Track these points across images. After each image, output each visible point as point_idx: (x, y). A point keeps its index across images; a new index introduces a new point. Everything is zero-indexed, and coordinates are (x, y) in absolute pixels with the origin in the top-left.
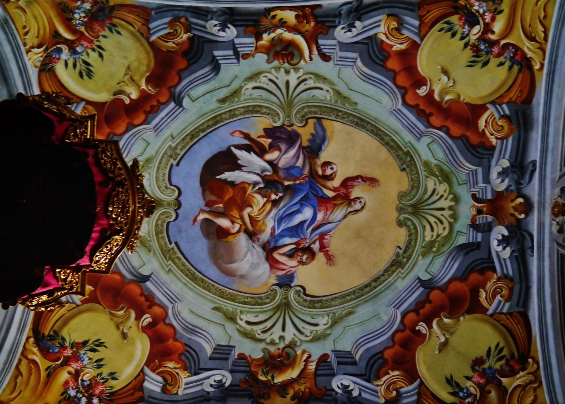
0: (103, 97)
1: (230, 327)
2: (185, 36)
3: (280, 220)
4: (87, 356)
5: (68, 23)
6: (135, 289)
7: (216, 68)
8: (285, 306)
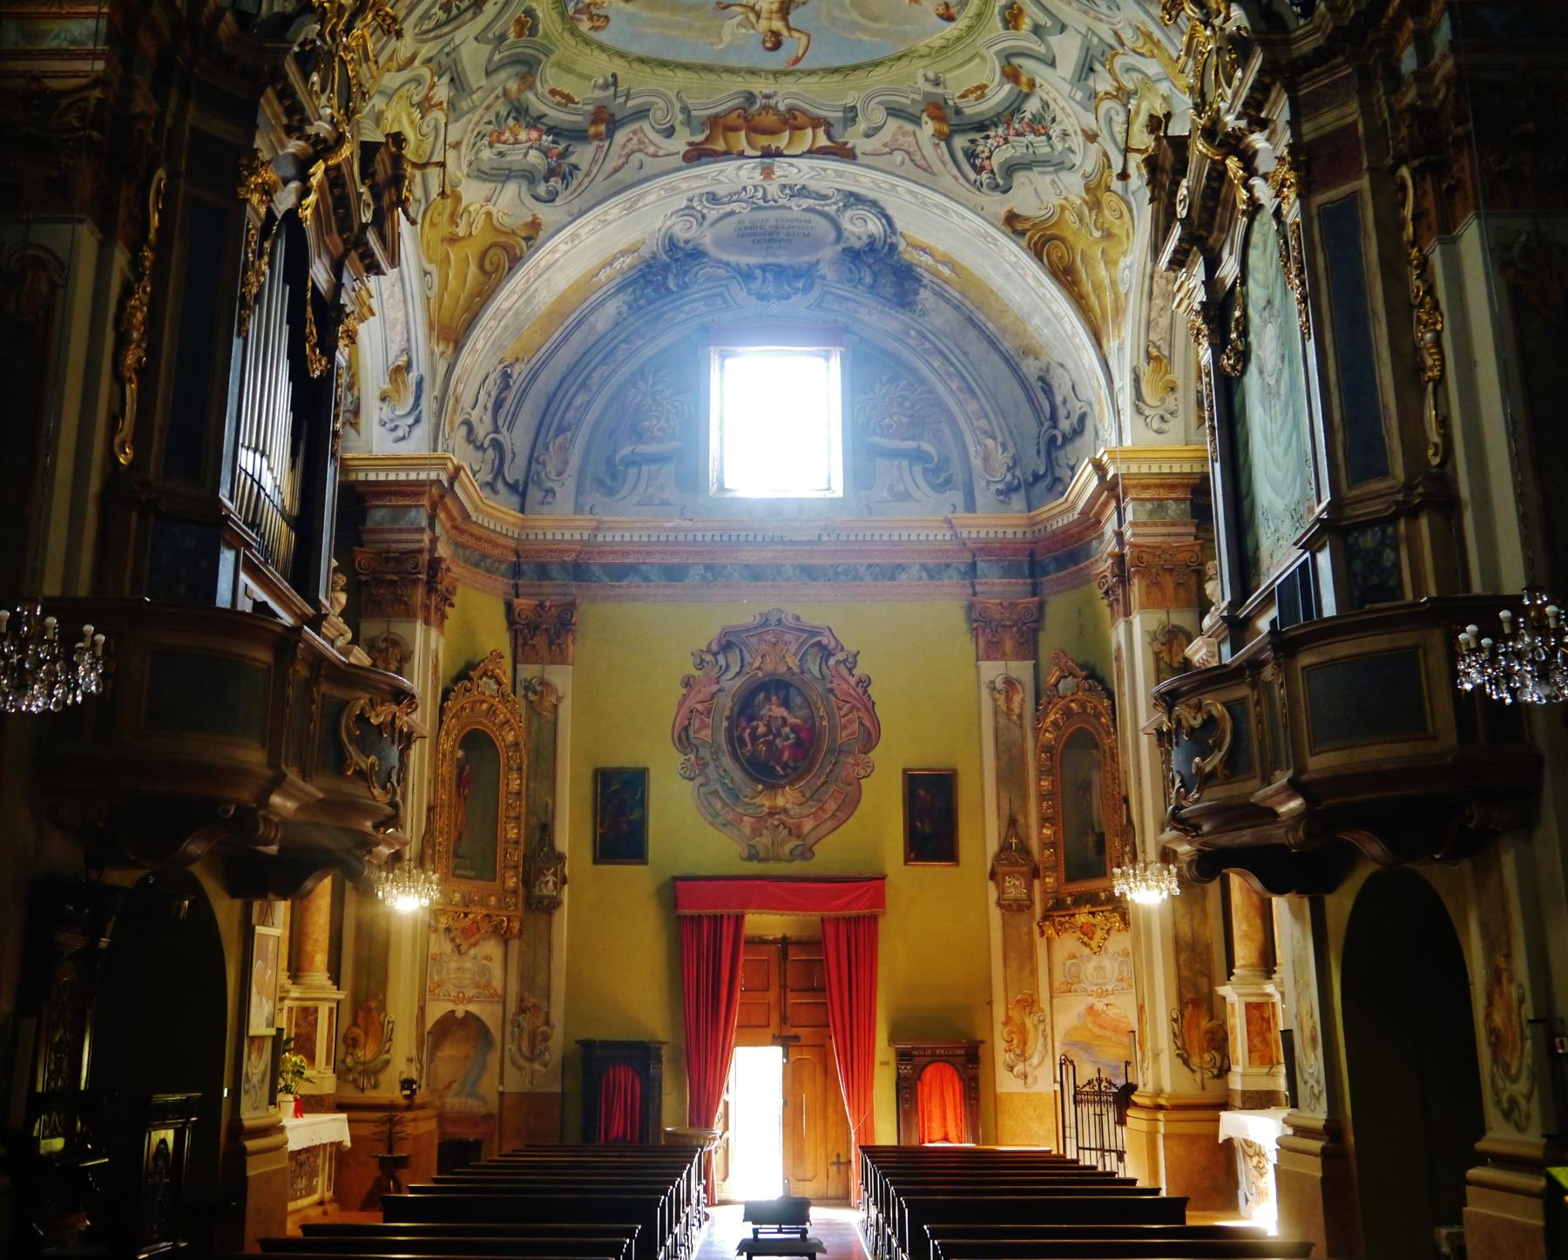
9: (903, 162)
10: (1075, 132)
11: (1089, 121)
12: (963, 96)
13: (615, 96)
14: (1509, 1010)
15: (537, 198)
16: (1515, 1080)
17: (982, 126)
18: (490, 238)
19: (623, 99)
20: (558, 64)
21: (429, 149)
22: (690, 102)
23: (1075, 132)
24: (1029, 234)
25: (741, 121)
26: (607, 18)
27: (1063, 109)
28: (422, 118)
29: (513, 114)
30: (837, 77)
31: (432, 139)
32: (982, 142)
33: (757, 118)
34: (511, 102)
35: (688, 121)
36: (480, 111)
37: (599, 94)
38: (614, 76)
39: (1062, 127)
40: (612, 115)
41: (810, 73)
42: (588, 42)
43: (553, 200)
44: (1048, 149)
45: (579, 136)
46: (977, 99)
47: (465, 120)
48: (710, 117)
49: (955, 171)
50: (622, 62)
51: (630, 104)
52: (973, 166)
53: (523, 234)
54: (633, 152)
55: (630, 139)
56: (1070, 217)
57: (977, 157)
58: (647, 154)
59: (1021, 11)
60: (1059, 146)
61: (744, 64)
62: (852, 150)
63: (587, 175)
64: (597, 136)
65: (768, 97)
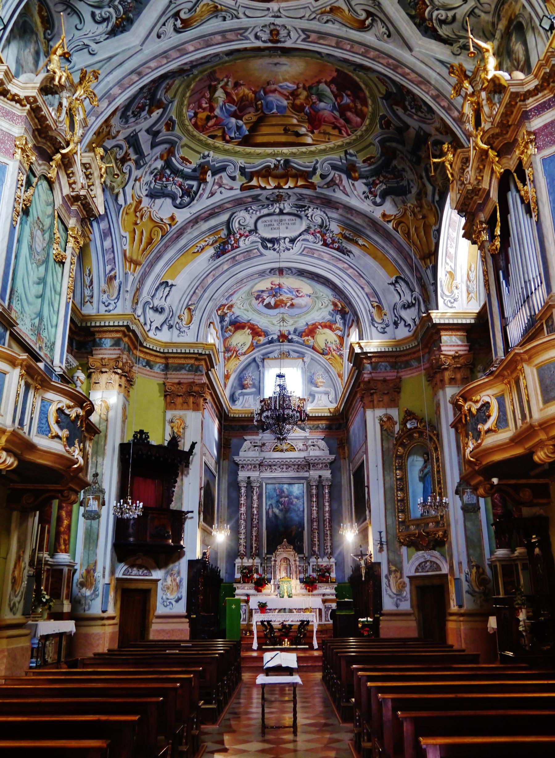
0: (251, 337)
1: (323, 310)
2: (230, 327)
4: (329, 345)
5: (231, 356)
6: (310, 327)
7: (238, 316)
8: (316, 297)
14: (20, 572)
16: (16, 597)
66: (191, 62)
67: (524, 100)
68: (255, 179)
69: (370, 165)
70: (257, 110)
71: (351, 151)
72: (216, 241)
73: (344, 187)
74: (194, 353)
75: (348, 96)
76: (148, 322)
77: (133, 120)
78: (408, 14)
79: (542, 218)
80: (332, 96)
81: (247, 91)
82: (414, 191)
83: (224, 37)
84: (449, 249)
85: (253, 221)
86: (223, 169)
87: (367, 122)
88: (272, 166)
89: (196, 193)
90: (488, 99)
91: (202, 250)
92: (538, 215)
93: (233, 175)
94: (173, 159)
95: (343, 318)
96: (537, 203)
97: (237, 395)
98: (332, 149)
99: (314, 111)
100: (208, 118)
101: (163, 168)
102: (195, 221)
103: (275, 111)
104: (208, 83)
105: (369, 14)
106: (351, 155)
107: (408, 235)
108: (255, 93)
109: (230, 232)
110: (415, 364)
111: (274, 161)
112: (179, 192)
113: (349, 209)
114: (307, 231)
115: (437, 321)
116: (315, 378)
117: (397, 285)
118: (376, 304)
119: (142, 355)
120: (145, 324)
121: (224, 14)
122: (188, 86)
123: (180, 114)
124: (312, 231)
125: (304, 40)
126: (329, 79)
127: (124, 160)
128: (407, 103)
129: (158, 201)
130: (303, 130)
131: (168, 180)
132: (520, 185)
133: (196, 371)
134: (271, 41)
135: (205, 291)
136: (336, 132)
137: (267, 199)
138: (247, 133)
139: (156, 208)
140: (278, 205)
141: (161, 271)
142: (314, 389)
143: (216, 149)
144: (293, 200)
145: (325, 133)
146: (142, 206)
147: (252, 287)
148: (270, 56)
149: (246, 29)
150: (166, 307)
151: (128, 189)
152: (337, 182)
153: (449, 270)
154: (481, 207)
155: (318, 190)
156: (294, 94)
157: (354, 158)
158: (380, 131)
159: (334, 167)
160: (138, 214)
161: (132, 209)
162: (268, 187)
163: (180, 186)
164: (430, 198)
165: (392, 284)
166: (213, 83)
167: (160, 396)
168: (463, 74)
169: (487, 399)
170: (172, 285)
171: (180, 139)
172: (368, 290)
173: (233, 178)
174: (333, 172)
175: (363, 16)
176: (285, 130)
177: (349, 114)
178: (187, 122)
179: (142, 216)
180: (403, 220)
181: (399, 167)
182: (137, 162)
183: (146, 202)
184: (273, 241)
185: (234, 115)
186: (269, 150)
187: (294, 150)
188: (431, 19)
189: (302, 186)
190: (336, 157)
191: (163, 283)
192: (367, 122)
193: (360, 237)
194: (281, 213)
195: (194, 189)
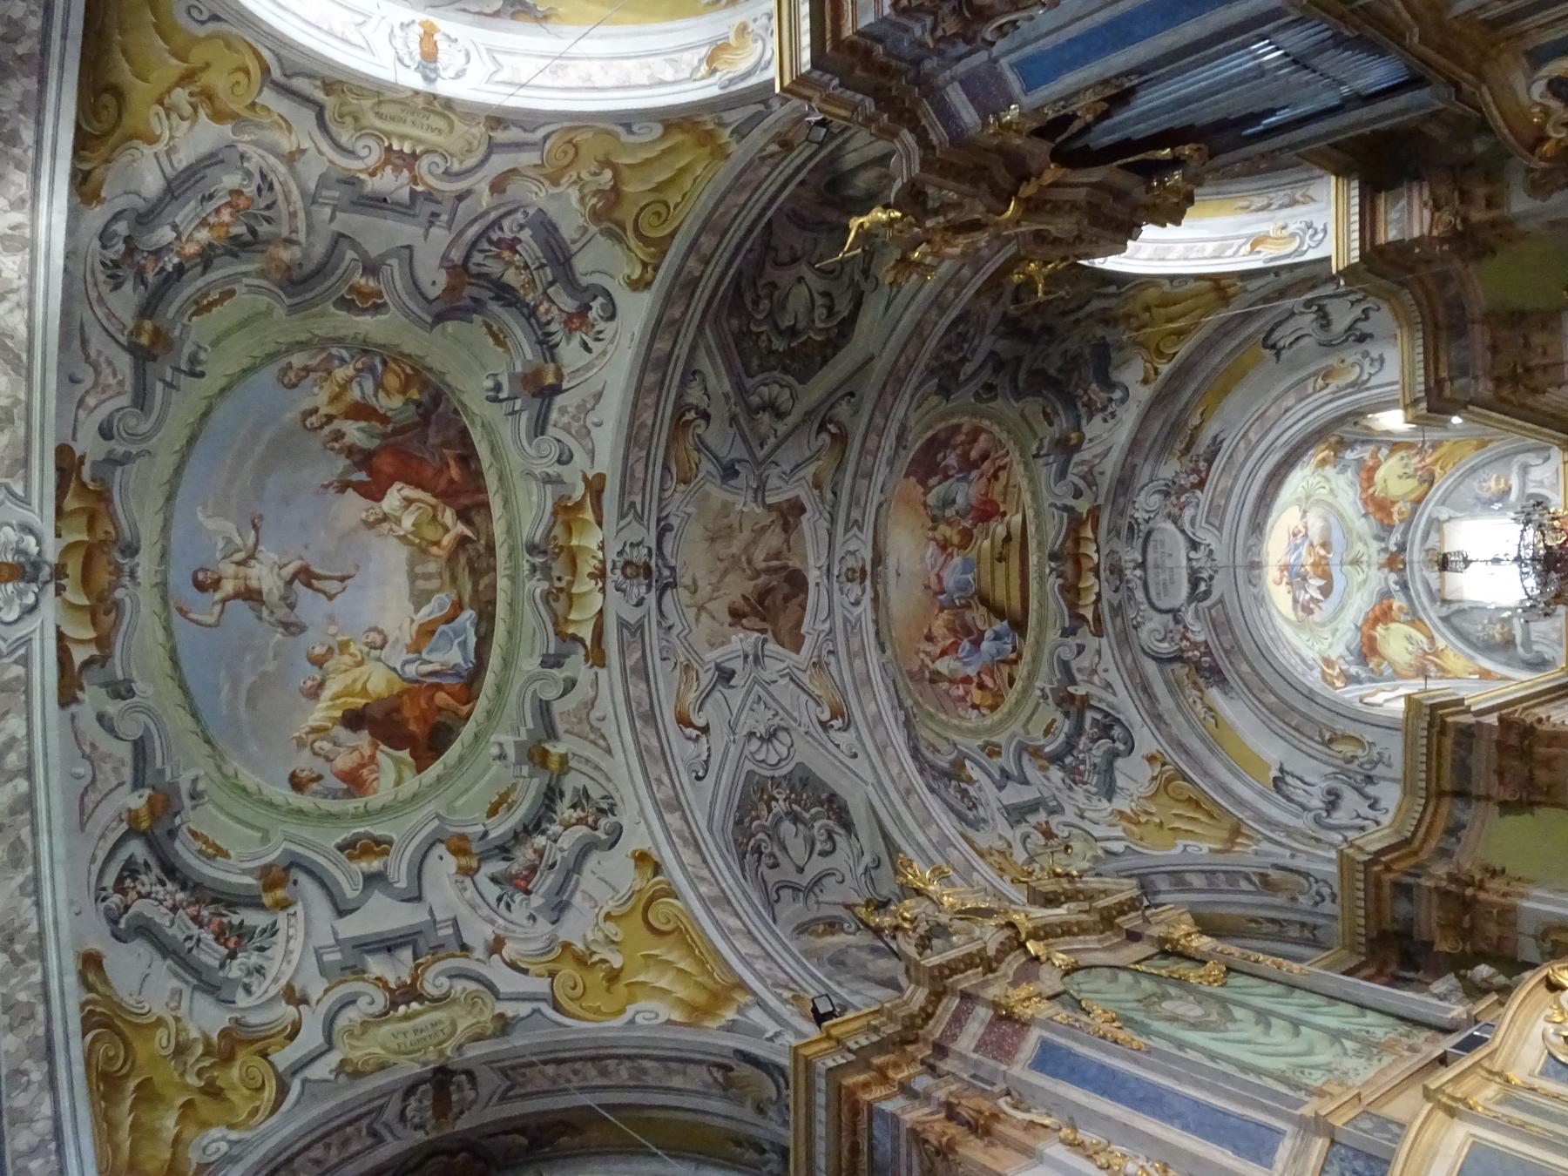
0: (1393, 626)
1: (1334, 485)
2: (1371, 665)
3: (1300, 556)
4: (1410, 471)
5: (1436, 665)
6: (1371, 509)
7: (1348, 649)
9: (79, 777)
10: (276, 980)
11: (316, 987)
12: (194, 834)
13: (177, 369)
15: (117, 217)
17: (171, 871)
18: (129, 122)
19: (168, 379)
20: (269, 311)
21: (333, 128)
22: (132, 468)
23: (276, 980)
24: (93, 995)
25: (101, 535)
26: (294, 386)
27: (287, 953)
28: (389, 149)
29: (248, 237)
30: (167, 664)
31: (344, 139)
32: (153, 878)
33: (105, 558)
34: (268, 242)
35: (112, 461)
36: (298, 203)
37: (187, 350)
38: (202, 375)
39: (265, 964)
40: (154, 358)
41: (168, 629)
42: (271, 357)
43: (101, 238)
44: (216, 964)
45: (147, 310)
46: (200, 852)
47: (312, 186)
48: (109, 490)
49: (101, 856)
50: (216, 388)
51: (159, 386)
52: (120, 879)
53: (96, 174)
54: (97, 373)
55: (115, 375)
56: (162, 1040)
57: (135, 880)
58: (87, 392)
59: (386, 853)
60: (235, 970)
61: (174, 545)
62: (75, 700)
63: (101, 300)
64: (138, 330)
65: (132, 575)
66: (893, 708)
67: (933, 148)
68: (1082, 611)
69: (1057, 413)
70: (968, 606)
71: (1034, 449)
72: (1195, 684)
73: (1095, 456)
74: (1429, 738)
75: (945, 458)
76: (1359, 822)
77: (981, 809)
78: (821, 368)
79: (1133, 63)
80: (946, 484)
81: (939, 622)
82: (1100, 331)
83: (856, 655)
84: (1206, 254)
85: (1158, 617)
86: (1065, 666)
87: (986, 423)
88: (1060, 581)
89: (1107, 715)
90: (936, 212)
91: (1210, 709)
92: (1127, 74)
93: (1075, 649)
94: (1047, 749)
95: (1350, 445)
96: (1105, 82)
97: (1528, 656)
98: (1031, 480)
99: (968, 513)
100: (981, 686)
101: (1063, 768)
102: (1157, 718)
103: (970, 577)
104: (926, 684)
105: (822, 428)
106: (1040, 448)
107: (1180, 334)
108: (942, 610)
109: (1178, 658)
110: (1453, 289)
111: (1052, 579)
112: (1105, 743)
113: (1135, 444)
114: (1175, 520)
115: (1356, 253)
116: (1487, 495)
117: (1281, 344)
118: (1320, 382)
119: (1433, 843)
120: (1362, 828)
121: (824, 653)
122: (931, 716)
123: (975, 732)
124: (1176, 511)
125: (861, 529)
126: (920, 489)
127: (1048, 834)
128: (954, 359)
129: (1121, 781)
130: (1001, 530)
131: (1083, 762)
132: (1076, 126)
133: (1472, 735)
134: (863, 580)
135: (1293, 709)
136: (1003, 475)
137: (1116, 590)
138: (1005, 623)
139: (1132, 787)
140: (1128, 572)
141: (1251, 787)
142: (1513, 496)
143: (1031, 676)
144: (1119, 545)
145: (1005, 494)
146: (1128, 811)
147: (1287, 620)
148: (886, 584)
149: (846, 620)
150: (1325, 785)
151: (1098, 832)
152: (1086, 469)
153: (1248, 247)
154: (1120, 195)
155: (1101, 501)
156: (944, 546)
157: (1046, 442)
158: (999, 400)
159: (1062, 474)
160: (1143, 819)
161: (1133, 828)
162: (1096, 589)
163: (1094, 741)
164: (1112, 302)
165: (1278, 355)
166: (927, 675)
167: (1532, 814)
168: (904, 262)
169: (1539, 88)
170: (1281, 770)
171: (1013, 736)
172: (1290, 401)
173: (1081, 649)
174: (1070, 477)
175: (825, 437)
176: (1000, 560)
177: (974, 454)
178: (988, 722)
179: (1146, 813)
180: (1153, 346)
181: (1059, 363)
182: (1052, 812)
183: (1121, 803)
184: (1194, 581)
185: (977, 643)
186: (1033, 586)
187: (1032, 545)
188: (827, 330)
189: (1095, 529)
190: (1045, 471)
191: (1276, 786)
192: (986, 423)
193: (1186, 422)
194: (1142, 565)
195: (1099, 716)
